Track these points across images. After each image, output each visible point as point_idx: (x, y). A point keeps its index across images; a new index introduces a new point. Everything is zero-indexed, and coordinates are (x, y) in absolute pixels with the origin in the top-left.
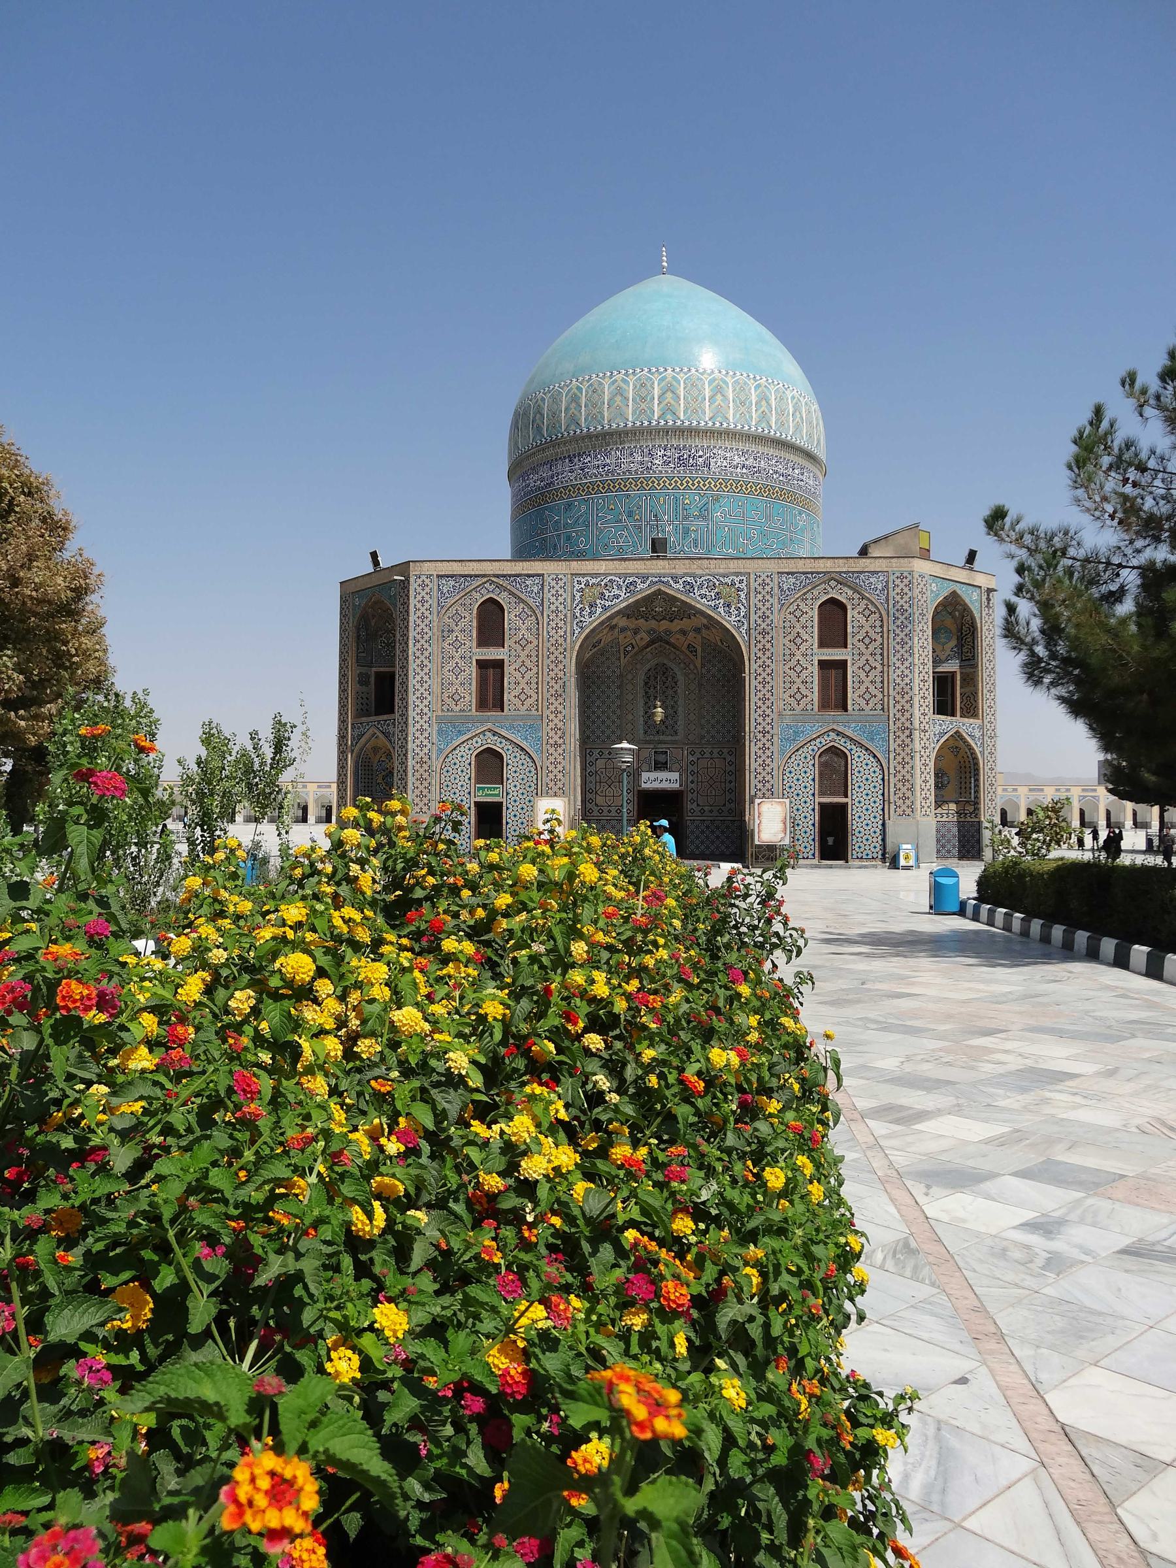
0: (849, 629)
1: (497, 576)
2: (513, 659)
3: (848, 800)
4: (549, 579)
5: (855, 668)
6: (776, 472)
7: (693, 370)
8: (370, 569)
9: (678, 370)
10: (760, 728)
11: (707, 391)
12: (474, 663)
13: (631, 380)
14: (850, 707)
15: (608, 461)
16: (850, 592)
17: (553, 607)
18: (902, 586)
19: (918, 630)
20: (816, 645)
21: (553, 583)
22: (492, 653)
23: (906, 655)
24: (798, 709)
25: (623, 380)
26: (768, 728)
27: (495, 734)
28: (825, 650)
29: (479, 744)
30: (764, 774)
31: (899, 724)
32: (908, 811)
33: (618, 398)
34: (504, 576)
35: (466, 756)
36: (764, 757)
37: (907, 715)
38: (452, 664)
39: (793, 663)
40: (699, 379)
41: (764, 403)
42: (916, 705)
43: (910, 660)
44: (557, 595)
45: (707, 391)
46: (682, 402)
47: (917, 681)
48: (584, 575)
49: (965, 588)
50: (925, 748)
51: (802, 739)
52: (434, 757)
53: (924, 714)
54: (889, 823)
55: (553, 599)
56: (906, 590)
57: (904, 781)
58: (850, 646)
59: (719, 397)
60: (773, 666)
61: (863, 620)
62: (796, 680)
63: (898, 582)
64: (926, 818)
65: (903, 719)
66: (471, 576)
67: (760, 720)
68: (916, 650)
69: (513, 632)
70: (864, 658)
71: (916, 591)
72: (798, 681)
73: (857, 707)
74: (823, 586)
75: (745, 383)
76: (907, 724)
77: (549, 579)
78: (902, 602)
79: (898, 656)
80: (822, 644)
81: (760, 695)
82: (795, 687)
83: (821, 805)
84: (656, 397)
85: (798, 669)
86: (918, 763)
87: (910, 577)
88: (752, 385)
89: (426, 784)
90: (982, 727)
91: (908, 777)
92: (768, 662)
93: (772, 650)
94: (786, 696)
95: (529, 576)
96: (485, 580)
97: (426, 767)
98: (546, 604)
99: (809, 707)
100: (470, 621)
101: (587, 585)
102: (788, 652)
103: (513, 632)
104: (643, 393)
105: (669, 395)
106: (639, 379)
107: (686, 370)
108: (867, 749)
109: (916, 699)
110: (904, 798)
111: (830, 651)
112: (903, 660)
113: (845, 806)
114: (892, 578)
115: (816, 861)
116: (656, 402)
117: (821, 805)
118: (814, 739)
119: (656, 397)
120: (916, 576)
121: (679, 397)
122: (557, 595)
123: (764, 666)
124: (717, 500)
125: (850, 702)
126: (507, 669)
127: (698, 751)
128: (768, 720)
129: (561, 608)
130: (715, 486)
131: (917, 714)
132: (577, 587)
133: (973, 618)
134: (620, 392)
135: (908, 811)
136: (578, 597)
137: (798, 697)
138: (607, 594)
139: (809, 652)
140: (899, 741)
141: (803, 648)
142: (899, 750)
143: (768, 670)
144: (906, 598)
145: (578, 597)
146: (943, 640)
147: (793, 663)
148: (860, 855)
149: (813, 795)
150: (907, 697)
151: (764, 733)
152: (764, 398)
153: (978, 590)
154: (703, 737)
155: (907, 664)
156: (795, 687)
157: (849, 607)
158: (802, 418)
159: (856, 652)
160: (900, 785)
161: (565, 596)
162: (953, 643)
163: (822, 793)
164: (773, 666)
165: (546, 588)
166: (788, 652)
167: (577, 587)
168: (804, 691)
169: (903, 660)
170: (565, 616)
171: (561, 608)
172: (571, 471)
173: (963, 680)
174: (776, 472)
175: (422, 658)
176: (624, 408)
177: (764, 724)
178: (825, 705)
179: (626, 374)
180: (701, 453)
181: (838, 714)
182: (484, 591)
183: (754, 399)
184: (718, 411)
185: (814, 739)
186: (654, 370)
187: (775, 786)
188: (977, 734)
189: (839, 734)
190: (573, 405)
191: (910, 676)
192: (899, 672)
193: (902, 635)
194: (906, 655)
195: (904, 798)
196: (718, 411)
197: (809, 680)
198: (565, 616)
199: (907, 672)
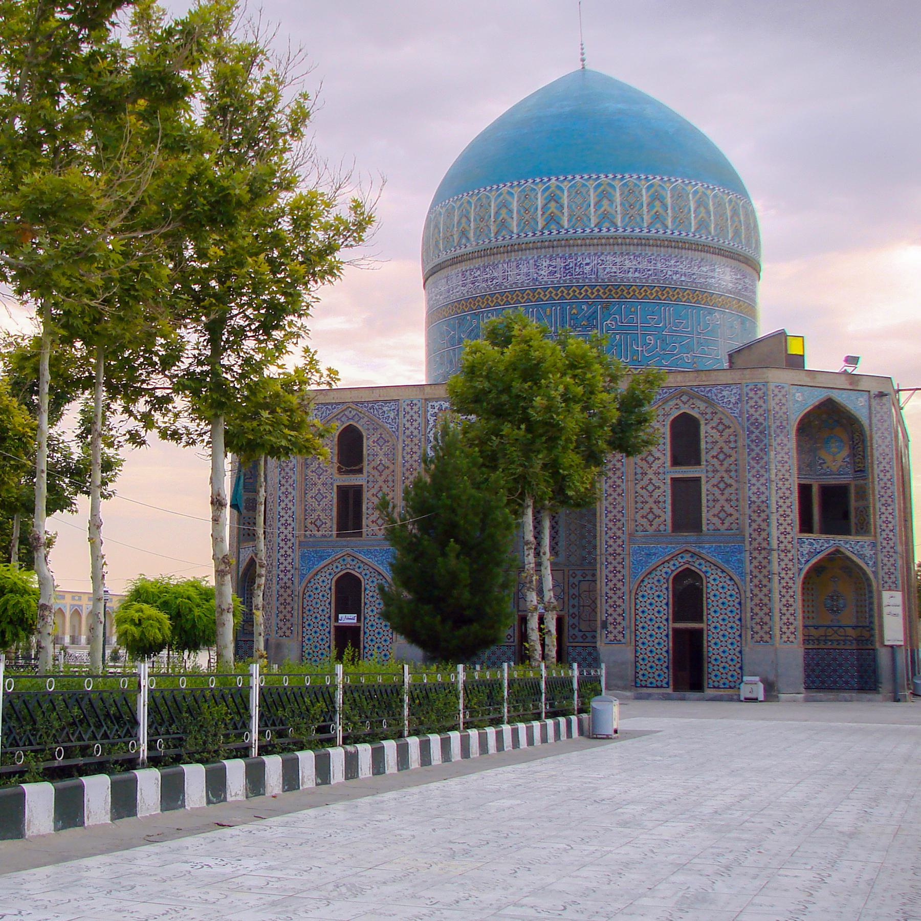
0: (703, 445)
1: (356, 403)
2: (371, 485)
3: (703, 626)
4: (404, 405)
5: (709, 487)
6: (676, 273)
7: (578, 177)
9: (562, 178)
10: (611, 550)
12: (335, 488)
14: (704, 528)
15: (496, 274)
16: (702, 406)
17: (408, 432)
18: (756, 398)
19: (774, 444)
20: (668, 464)
21: (408, 409)
23: (762, 472)
24: (651, 530)
26: (619, 550)
27: (354, 558)
28: (678, 468)
29: (339, 570)
30: (615, 598)
31: (755, 544)
32: (766, 638)
33: (504, 212)
34: (362, 403)
35: (326, 584)
36: (614, 581)
37: (764, 534)
38: (314, 491)
39: (645, 482)
40: (584, 185)
41: (657, 203)
42: (774, 524)
43: (766, 476)
44: (412, 421)
46: (566, 210)
47: (774, 499)
48: (437, 400)
49: (845, 394)
50: (786, 569)
51: (654, 561)
52: (296, 581)
53: (785, 533)
54: (746, 649)
55: (408, 425)
56: (761, 402)
57: (761, 605)
58: (704, 463)
59: (605, 202)
60: (624, 486)
61: (716, 435)
62: (648, 499)
63: (751, 394)
64: (789, 645)
65: (760, 539)
66: (332, 404)
67: (611, 542)
68: (773, 467)
69: (371, 458)
70: (719, 475)
71: (772, 404)
72: (651, 501)
73: (711, 527)
74: (675, 402)
75: (636, 185)
76: (764, 545)
77: (404, 405)
78: (756, 415)
79: (754, 472)
80: (676, 462)
81: (610, 516)
82: (647, 506)
83: (675, 631)
84: (539, 207)
85: (650, 488)
86: (776, 585)
87: (764, 389)
88: (644, 185)
89: (289, 608)
90: (874, 545)
91: (766, 600)
92: (619, 482)
93: (623, 469)
94: (638, 516)
95: (386, 402)
96: (344, 407)
97: (289, 591)
98: (401, 429)
99: (662, 528)
101: (440, 409)
102: (639, 471)
103: (371, 458)
104: (527, 204)
105: (553, 205)
106: (523, 190)
107: (570, 177)
108: (723, 571)
109: (774, 518)
110: (762, 624)
111: (684, 468)
112: (758, 476)
113: (700, 632)
114: (745, 390)
115: (670, 691)
116: (539, 213)
117: (675, 631)
118: (668, 561)
119: (539, 207)
120: (771, 386)
121: (562, 206)
122: (412, 421)
123: (615, 487)
124: (607, 308)
125: (704, 522)
126: (366, 495)
127: (579, 573)
128: (619, 542)
129: (416, 432)
130: (604, 293)
131: (775, 533)
132: (431, 411)
133: (861, 426)
134: (505, 205)
135: (766, 638)
136: (431, 422)
137: (650, 517)
139: (661, 470)
140: (755, 563)
141: (655, 466)
142: (756, 572)
143: (619, 490)
144: (761, 411)
145: (431, 422)
146: (834, 450)
147: (645, 482)
148: (716, 684)
149: (667, 620)
150: (763, 515)
151: (615, 554)
152: (657, 197)
153: (866, 395)
154: (584, 558)
155: (762, 480)
156: (647, 506)
157: (702, 422)
158: (708, 212)
159: (710, 468)
160: (756, 610)
161: (419, 420)
162: (845, 452)
163: (675, 620)
164: (624, 486)
165: (401, 414)
166: (639, 471)
167: (431, 411)
168: (657, 511)
169: (758, 476)
170: (420, 440)
171: (416, 432)
172: (464, 285)
173: (857, 494)
174: (676, 273)
175: (287, 486)
176: (509, 220)
177: (615, 546)
178: (678, 526)
180: (588, 261)
181: (691, 536)
182: (344, 419)
183: (645, 199)
184: (605, 216)
185: (668, 561)
186: (538, 180)
187: (627, 611)
188: (868, 552)
189: (694, 554)
190: (464, 220)
191: (767, 493)
192: (754, 489)
193: (757, 450)
194: (762, 472)
195: (762, 624)
196: (605, 216)
197: (661, 499)
198: (420, 440)
199: (763, 489)
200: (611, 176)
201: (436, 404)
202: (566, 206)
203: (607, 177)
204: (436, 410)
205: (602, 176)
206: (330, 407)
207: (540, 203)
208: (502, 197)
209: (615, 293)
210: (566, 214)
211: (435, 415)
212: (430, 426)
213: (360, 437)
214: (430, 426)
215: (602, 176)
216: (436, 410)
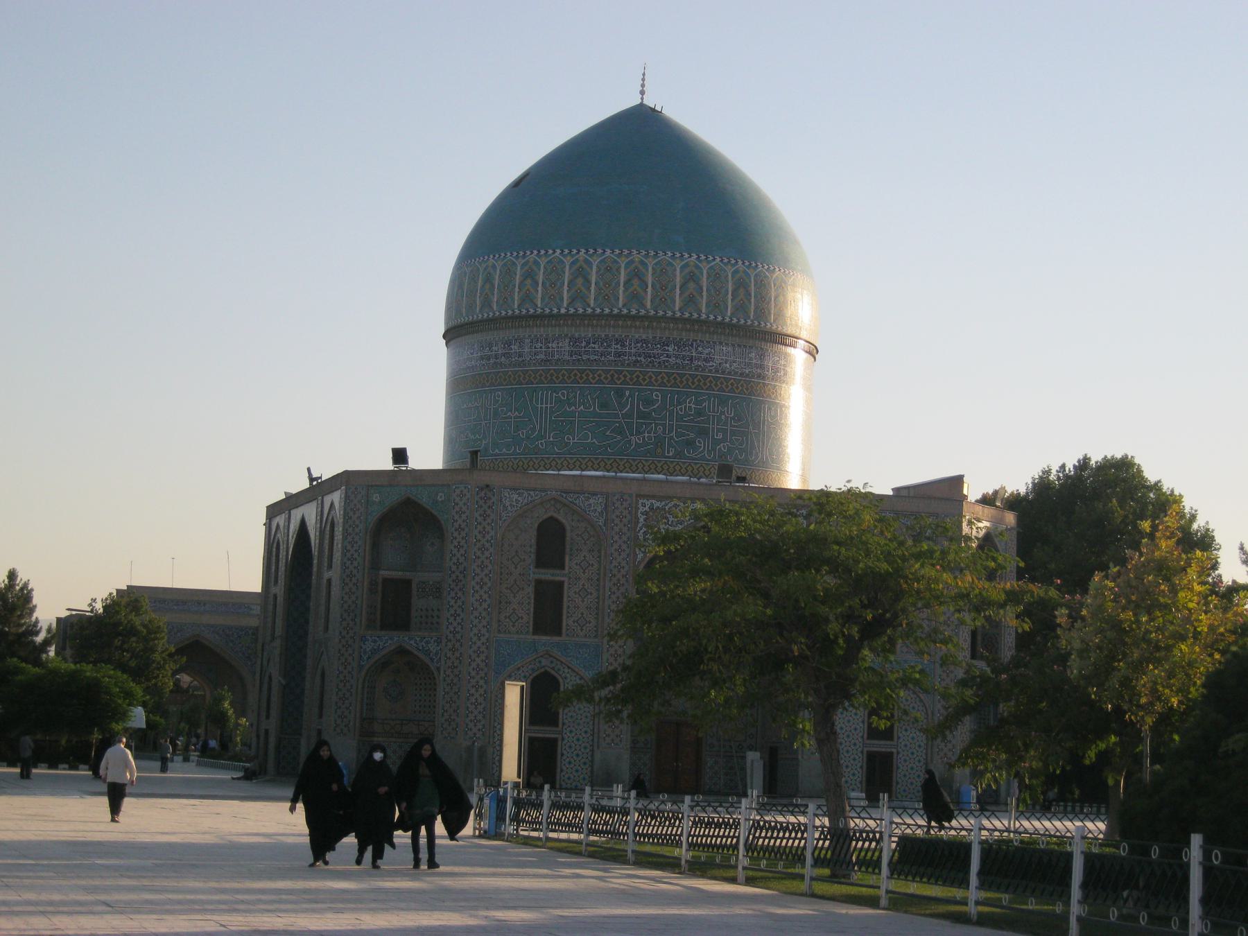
8: (387, 464)
11: (730, 284)
13: (651, 263)
22: (548, 575)
25: (642, 263)
33: (636, 282)
45: (730, 284)
48: (648, 497)
100: (530, 538)
101: (651, 508)
105: (691, 285)
121: (701, 288)
138: (671, 519)
145: (641, 520)
149: (862, 737)
167: (641, 509)
179: (647, 255)
200: (747, 263)
201: (648, 503)
202: (705, 289)
203: (743, 263)
204: (647, 508)
205: (740, 262)
206: (532, 493)
207: (678, 280)
208: (633, 266)
209: (747, 389)
210: (705, 297)
211: (646, 513)
212: (640, 525)
213: (562, 528)
214: (640, 525)
215: (740, 262)
216: (647, 508)
